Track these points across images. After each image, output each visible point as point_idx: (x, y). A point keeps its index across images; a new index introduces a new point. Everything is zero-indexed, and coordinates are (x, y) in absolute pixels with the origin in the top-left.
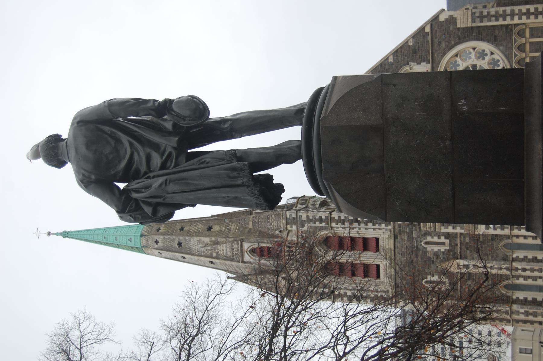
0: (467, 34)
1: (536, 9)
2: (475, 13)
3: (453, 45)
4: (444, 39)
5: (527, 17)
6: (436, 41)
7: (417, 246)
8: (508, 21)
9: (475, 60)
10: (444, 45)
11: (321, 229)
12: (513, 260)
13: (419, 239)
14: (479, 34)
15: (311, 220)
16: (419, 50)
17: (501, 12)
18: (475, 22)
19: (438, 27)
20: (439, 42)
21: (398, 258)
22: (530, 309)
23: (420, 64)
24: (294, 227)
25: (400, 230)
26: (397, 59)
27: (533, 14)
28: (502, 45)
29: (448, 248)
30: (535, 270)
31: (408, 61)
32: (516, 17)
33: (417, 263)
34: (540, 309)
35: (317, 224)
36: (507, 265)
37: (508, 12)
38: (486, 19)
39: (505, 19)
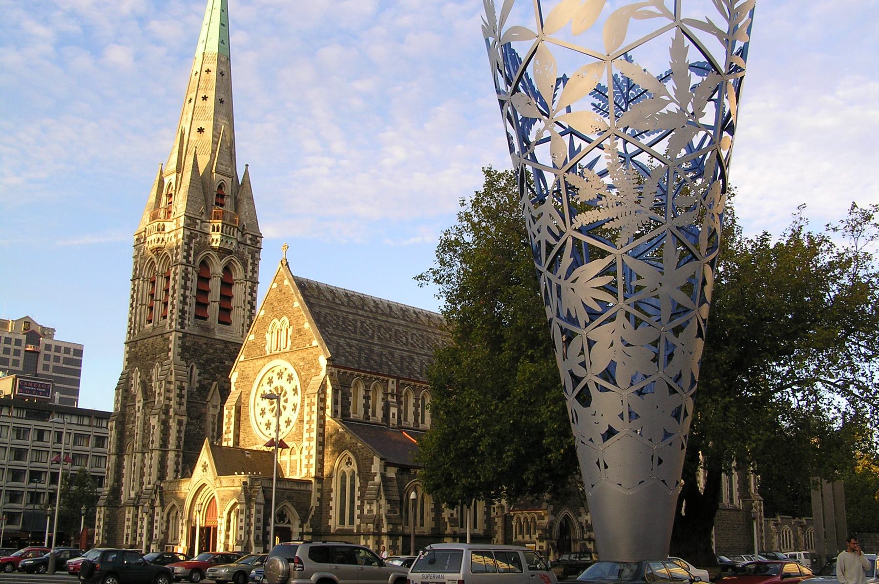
7: (156, 359)
8: (306, 435)
11: (172, 258)
19: (316, 355)
21: (151, 340)
22: (111, 472)
24: (174, 228)
33: (147, 360)
34: (111, 481)
35: (175, 251)
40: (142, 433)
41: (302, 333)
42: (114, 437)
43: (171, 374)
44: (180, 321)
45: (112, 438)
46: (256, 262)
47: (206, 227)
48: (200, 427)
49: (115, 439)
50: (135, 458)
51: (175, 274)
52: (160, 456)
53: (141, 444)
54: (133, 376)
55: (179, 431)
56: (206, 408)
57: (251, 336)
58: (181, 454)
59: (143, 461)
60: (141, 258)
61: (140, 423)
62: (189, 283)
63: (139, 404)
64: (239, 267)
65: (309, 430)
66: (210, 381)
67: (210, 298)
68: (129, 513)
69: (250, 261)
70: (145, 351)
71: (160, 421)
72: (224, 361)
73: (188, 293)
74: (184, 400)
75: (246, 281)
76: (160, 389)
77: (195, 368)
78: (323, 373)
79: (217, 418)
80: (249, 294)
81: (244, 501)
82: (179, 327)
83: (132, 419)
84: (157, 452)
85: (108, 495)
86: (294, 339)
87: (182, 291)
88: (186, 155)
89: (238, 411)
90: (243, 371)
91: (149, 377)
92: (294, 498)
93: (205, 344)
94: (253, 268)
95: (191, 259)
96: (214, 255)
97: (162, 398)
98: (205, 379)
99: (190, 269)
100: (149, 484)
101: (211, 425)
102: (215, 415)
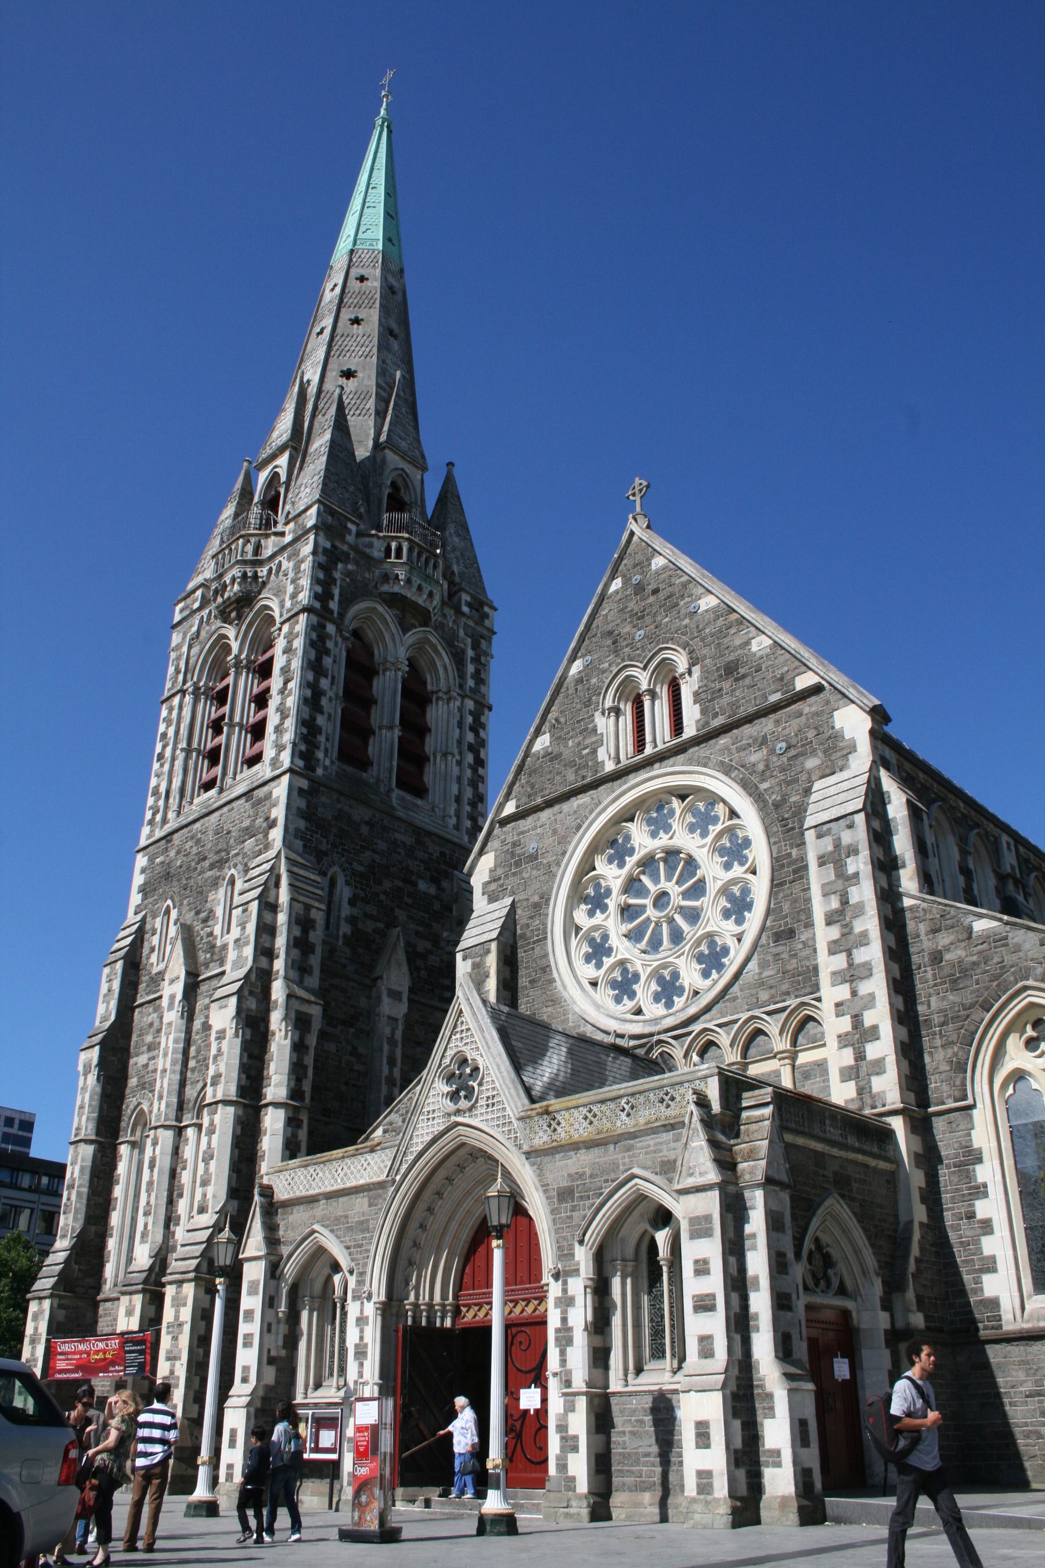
0: (793, 828)
1: (878, 1067)
2: (850, 826)
3: (757, 788)
4: (772, 751)
5: (847, 1034)
6: (766, 726)
8: (828, 964)
9: (719, 883)
10: (754, 758)
12: (179, 1131)
13: (240, 858)
14: (795, 872)
15: (297, 569)
16: (737, 680)
17: (858, 927)
18: (819, 836)
19: (817, 714)
20: (765, 737)
23: (695, 702)
25: (260, 802)
26: (709, 623)
27: (860, 1056)
28: (763, 965)
29: (219, 943)
30: (149, 1196)
31: (705, 658)
32: (843, 992)
33: (202, 872)
34: (75, 1219)
35: (290, 589)
36: (166, 1115)
37: (861, 956)
38: (833, 877)
39: (834, 948)
40: (178, 1067)
41: (742, 671)
42: (93, 1091)
43: (277, 885)
44: (303, 748)
45: (87, 1096)
46: (483, 659)
47: (370, 545)
48: (355, 1048)
49: (97, 1097)
50: (155, 1143)
51: (290, 637)
52: (238, 1121)
53: (175, 1100)
54: (158, 925)
55: (298, 1047)
56: (369, 997)
57: (539, 740)
58: (304, 1117)
59: (176, 1151)
60: (190, 647)
61: (176, 1041)
62: (327, 661)
63: (173, 989)
64: (444, 660)
65: (845, 945)
66: (381, 925)
67: (377, 717)
68: (129, 1313)
69: (470, 653)
70: (195, 850)
71: (243, 1015)
72: (414, 878)
73: (324, 683)
74: (315, 961)
75: (463, 697)
76: (243, 926)
77: (341, 880)
78: (862, 759)
79: (400, 1027)
80: (471, 729)
82: (301, 763)
83: (149, 1039)
84: (231, 1110)
85: (67, 1261)
86: (704, 698)
87: (310, 676)
88: (313, 416)
89: (509, 961)
90: (515, 844)
91: (203, 915)
93: (367, 823)
94: (477, 672)
95: (334, 605)
96: (387, 616)
97: (249, 951)
98: (367, 915)
99: (331, 628)
100: (202, 1210)
101: (386, 1047)
102: (396, 1020)
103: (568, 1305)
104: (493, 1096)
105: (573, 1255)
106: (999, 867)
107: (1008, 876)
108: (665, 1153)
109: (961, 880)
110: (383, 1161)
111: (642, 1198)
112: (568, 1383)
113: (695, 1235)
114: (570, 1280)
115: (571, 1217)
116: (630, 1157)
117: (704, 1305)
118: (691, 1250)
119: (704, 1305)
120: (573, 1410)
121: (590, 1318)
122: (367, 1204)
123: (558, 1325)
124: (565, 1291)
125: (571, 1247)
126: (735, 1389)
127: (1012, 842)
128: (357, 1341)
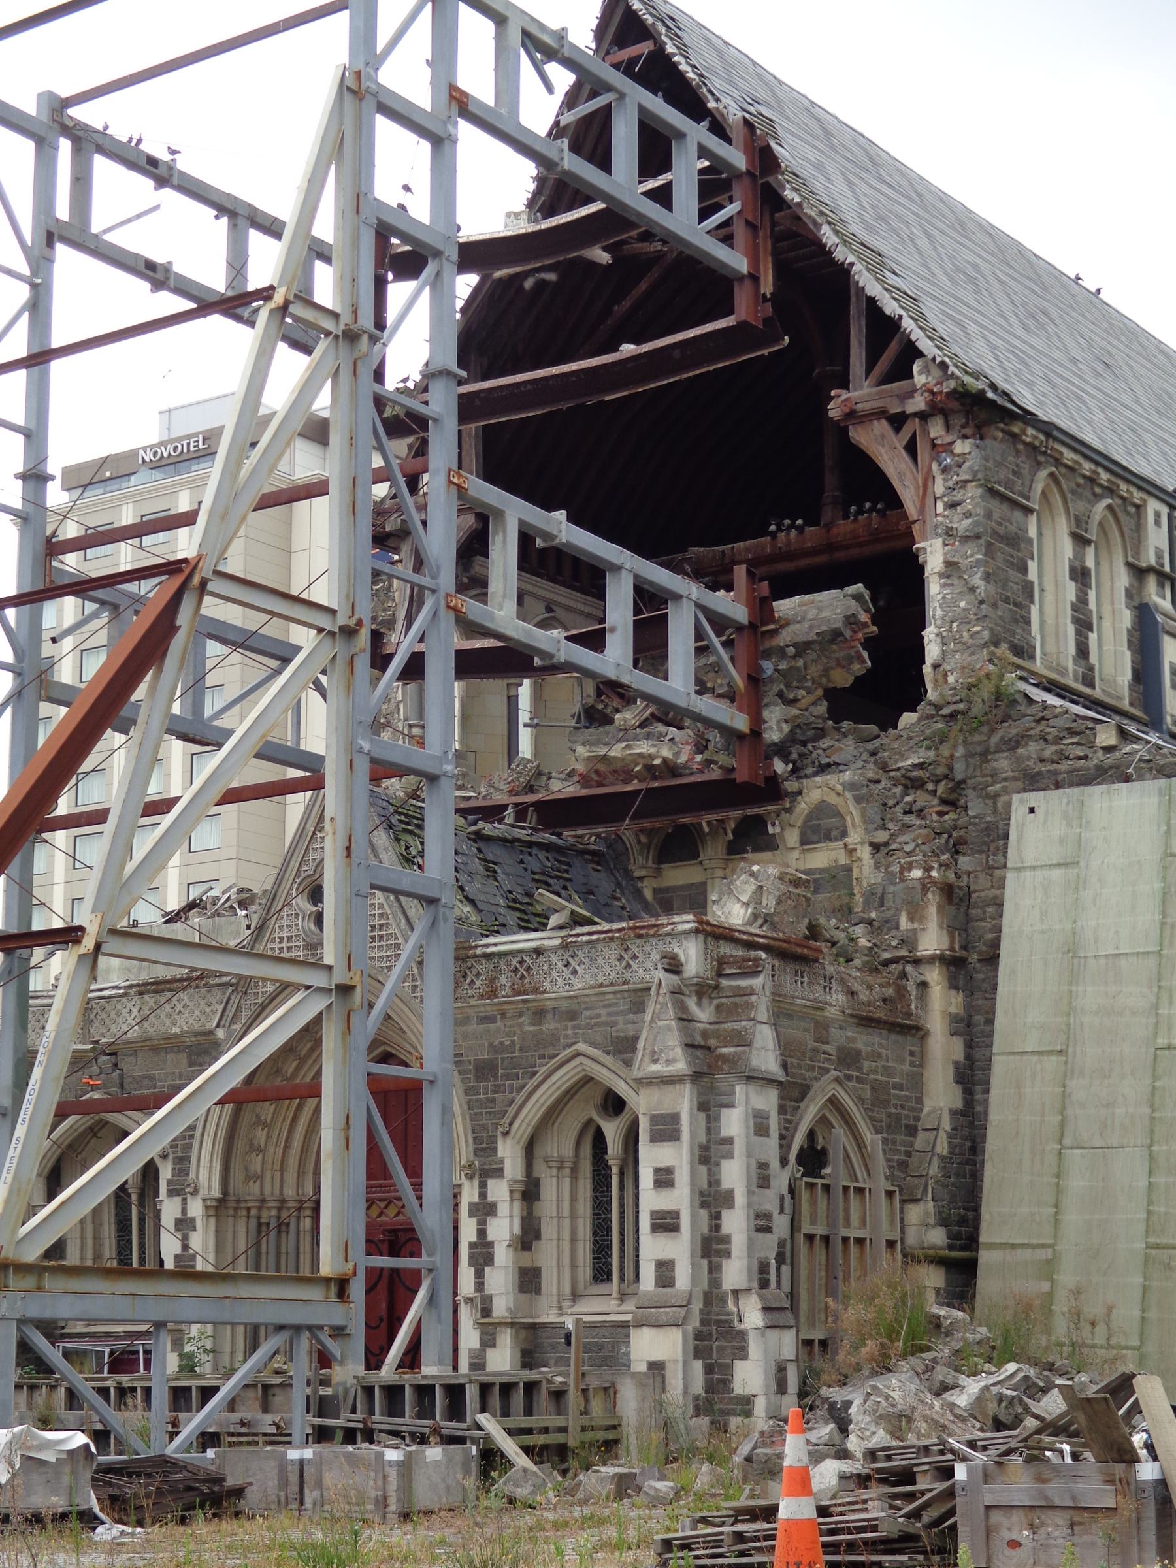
81: (681, 1066)
92: (866, 1065)
103: (488, 1214)
104: (381, 926)
105: (495, 1150)
106: (1137, 554)
107: (1150, 569)
108: (621, 1026)
109: (1070, 591)
110: (209, 1004)
111: (588, 1080)
112: (486, 1312)
113: (657, 1137)
114: (491, 1183)
115: (493, 1100)
116: (574, 1028)
117: (666, 1223)
118: (651, 1156)
119: (666, 1223)
120: (493, 1346)
121: (517, 1230)
122: (185, 1061)
123: (474, 1239)
124: (483, 1195)
125: (493, 1140)
126: (698, 1324)
127: (1165, 510)
128: (179, 1251)
